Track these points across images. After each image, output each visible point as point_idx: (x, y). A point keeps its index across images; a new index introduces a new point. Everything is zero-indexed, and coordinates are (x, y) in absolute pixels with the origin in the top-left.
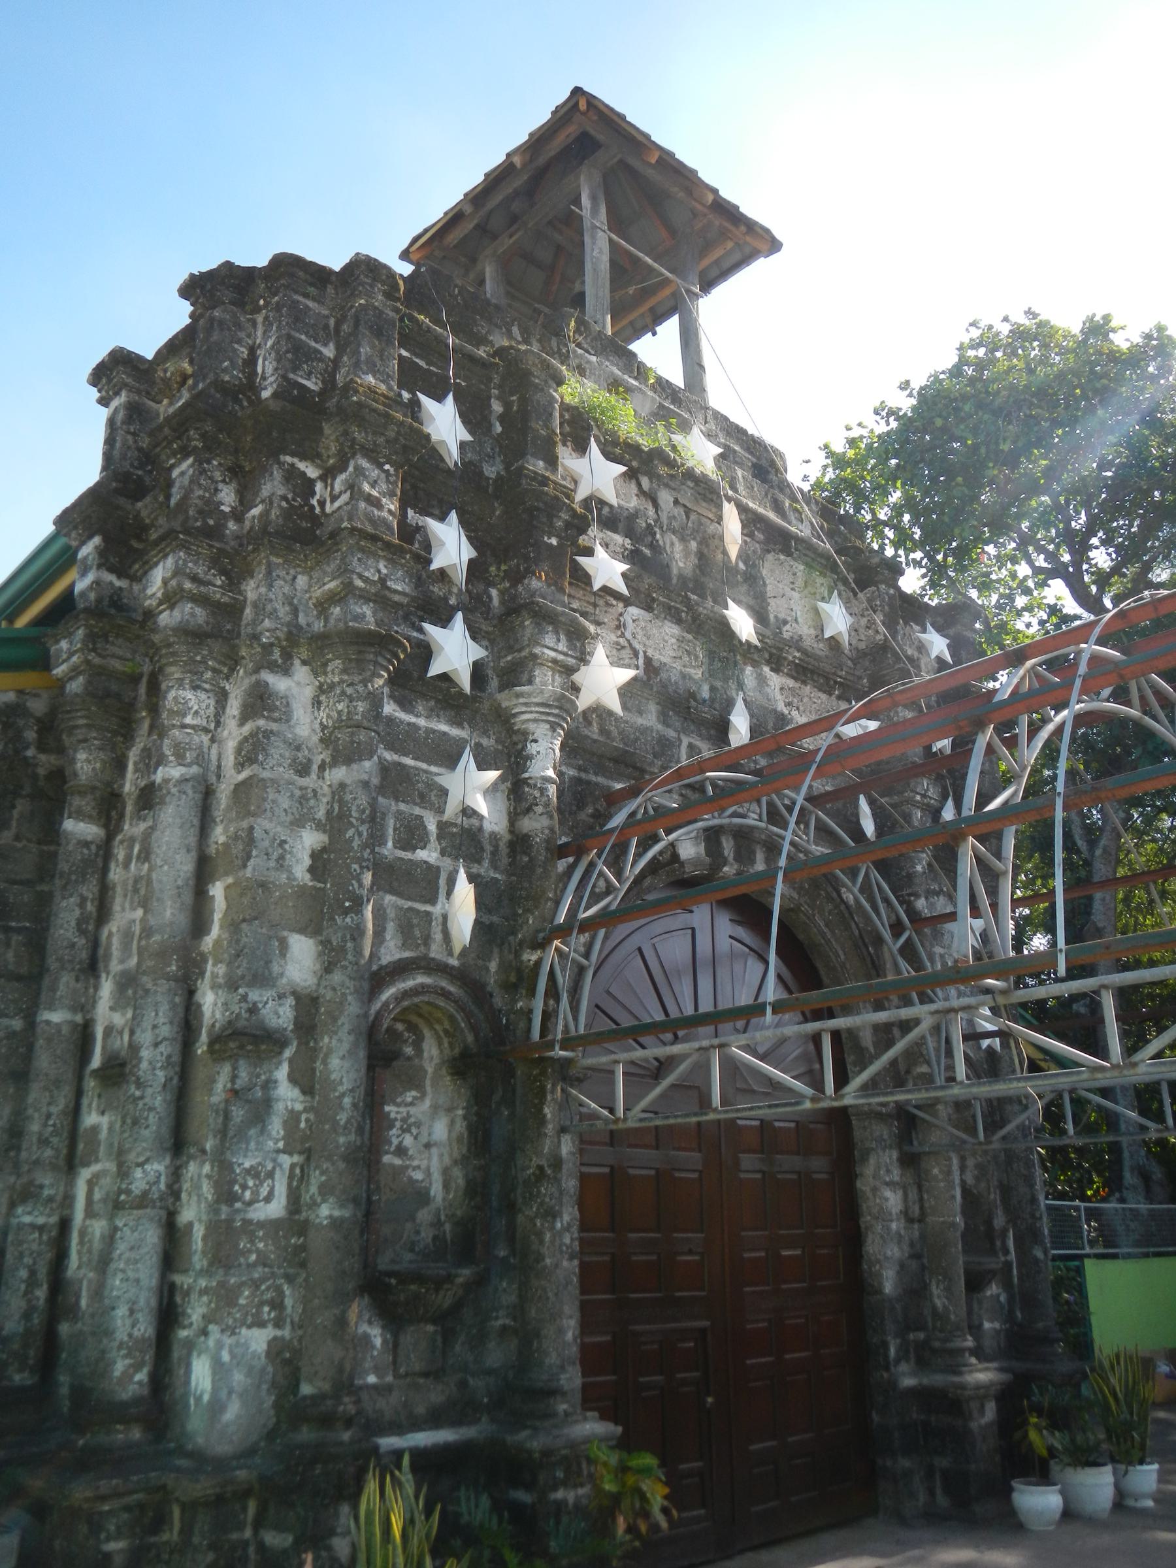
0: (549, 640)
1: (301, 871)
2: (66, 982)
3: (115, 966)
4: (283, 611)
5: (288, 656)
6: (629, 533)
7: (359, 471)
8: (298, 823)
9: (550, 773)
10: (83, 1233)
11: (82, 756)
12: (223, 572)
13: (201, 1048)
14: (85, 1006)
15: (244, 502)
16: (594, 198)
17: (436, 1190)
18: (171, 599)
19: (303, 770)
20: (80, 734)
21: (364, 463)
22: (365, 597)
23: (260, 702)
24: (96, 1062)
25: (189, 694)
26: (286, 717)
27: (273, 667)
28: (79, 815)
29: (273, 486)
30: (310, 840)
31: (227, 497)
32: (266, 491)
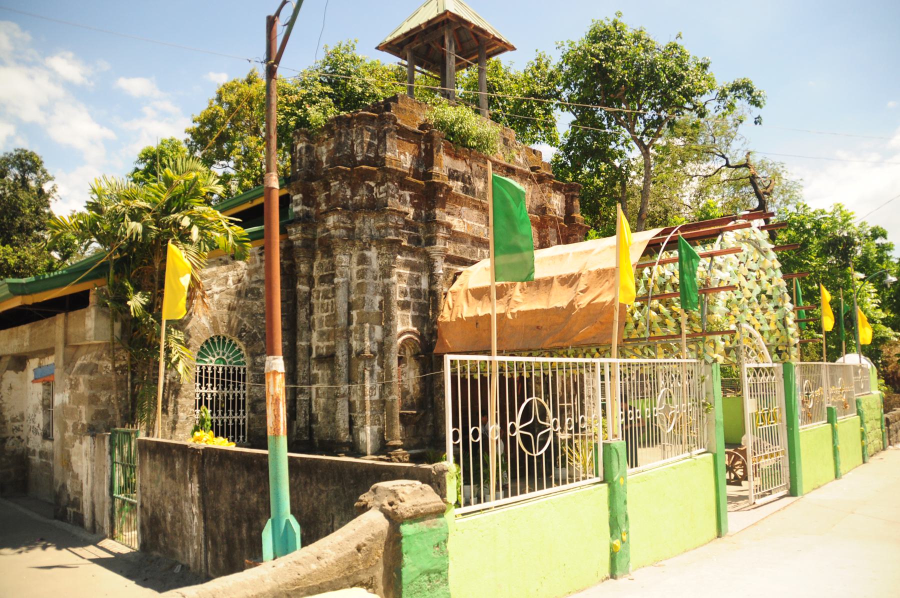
0: (441, 230)
1: (377, 309)
2: (305, 333)
3: (317, 328)
4: (368, 231)
5: (370, 245)
6: (463, 181)
7: (388, 187)
8: (375, 294)
9: (441, 271)
10: (316, 402)
11: (302, 266)
12: (350, 219)
13: (353, 355)
14: (309, 340)
15: (354, 195)
16: (450, 42)
17: (411, 390)
18: (335, 228)
19: (375, 279)
20: (301, 259)
21: (390, 184)
22: (391, 227)
23: (363, 260)
24: (314, 355)
25: (343, 257)
26: (370, 264)
27: (366, 249)
28: (302, 284)
29: (363, 191)
30: (378, 298)
31: (349, 193)
32: (361, 192)
